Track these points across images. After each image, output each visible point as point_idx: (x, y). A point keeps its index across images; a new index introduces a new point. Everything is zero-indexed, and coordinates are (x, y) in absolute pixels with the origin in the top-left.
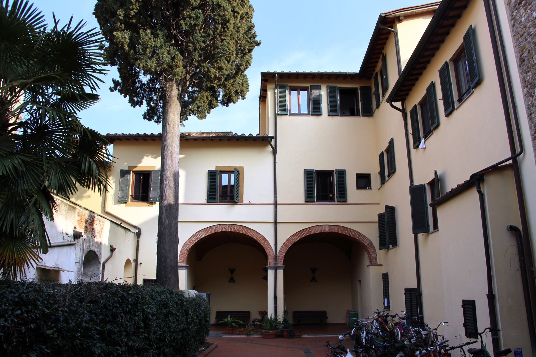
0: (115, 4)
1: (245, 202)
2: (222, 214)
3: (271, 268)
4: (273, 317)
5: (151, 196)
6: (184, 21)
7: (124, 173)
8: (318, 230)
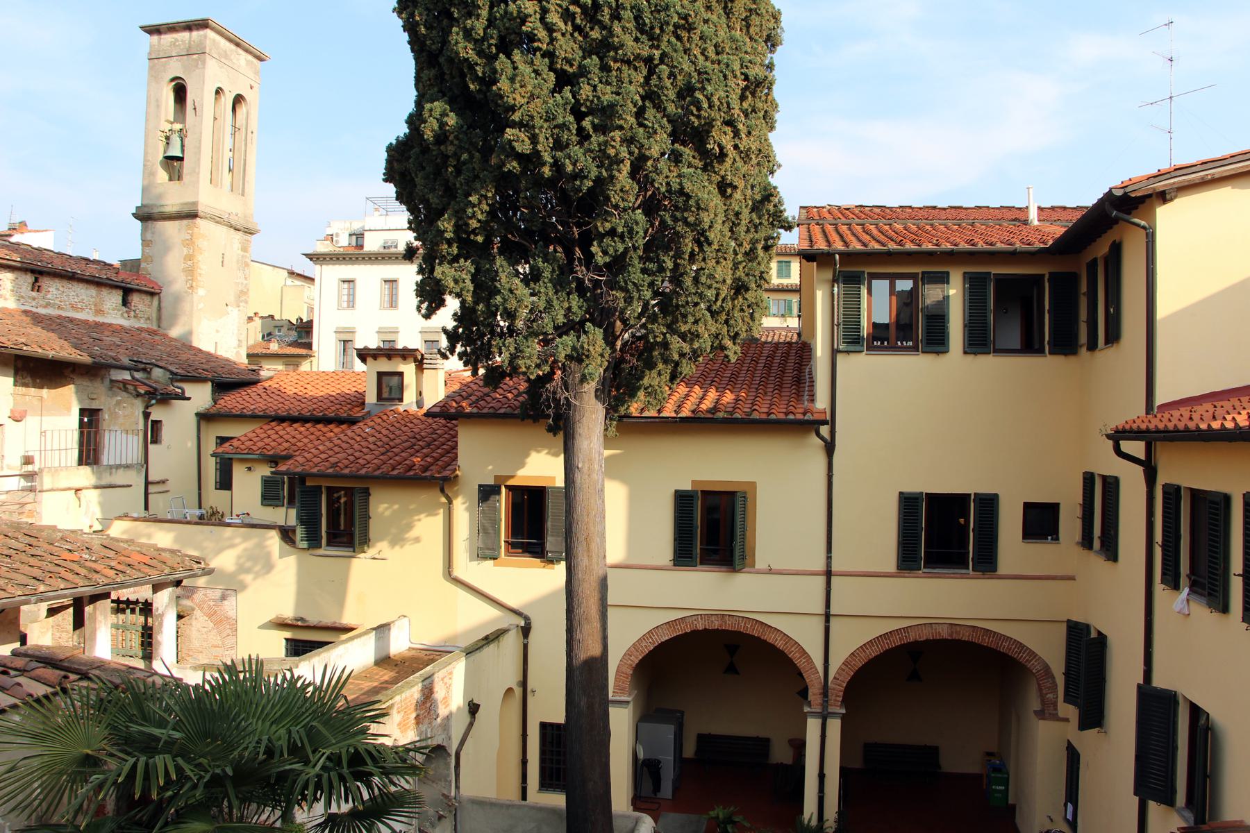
0: (433, 190)
1: (760, 564)
2: (707, 593)
3: (814, 715)
4: (814, 823)
5: (548, 547)
6: (600, 246)
7: (487, 493)
8: (925, 635)
